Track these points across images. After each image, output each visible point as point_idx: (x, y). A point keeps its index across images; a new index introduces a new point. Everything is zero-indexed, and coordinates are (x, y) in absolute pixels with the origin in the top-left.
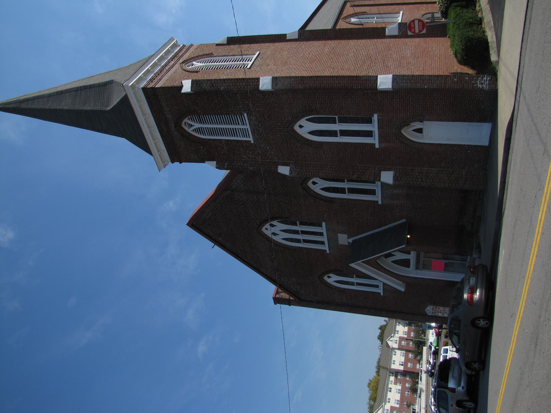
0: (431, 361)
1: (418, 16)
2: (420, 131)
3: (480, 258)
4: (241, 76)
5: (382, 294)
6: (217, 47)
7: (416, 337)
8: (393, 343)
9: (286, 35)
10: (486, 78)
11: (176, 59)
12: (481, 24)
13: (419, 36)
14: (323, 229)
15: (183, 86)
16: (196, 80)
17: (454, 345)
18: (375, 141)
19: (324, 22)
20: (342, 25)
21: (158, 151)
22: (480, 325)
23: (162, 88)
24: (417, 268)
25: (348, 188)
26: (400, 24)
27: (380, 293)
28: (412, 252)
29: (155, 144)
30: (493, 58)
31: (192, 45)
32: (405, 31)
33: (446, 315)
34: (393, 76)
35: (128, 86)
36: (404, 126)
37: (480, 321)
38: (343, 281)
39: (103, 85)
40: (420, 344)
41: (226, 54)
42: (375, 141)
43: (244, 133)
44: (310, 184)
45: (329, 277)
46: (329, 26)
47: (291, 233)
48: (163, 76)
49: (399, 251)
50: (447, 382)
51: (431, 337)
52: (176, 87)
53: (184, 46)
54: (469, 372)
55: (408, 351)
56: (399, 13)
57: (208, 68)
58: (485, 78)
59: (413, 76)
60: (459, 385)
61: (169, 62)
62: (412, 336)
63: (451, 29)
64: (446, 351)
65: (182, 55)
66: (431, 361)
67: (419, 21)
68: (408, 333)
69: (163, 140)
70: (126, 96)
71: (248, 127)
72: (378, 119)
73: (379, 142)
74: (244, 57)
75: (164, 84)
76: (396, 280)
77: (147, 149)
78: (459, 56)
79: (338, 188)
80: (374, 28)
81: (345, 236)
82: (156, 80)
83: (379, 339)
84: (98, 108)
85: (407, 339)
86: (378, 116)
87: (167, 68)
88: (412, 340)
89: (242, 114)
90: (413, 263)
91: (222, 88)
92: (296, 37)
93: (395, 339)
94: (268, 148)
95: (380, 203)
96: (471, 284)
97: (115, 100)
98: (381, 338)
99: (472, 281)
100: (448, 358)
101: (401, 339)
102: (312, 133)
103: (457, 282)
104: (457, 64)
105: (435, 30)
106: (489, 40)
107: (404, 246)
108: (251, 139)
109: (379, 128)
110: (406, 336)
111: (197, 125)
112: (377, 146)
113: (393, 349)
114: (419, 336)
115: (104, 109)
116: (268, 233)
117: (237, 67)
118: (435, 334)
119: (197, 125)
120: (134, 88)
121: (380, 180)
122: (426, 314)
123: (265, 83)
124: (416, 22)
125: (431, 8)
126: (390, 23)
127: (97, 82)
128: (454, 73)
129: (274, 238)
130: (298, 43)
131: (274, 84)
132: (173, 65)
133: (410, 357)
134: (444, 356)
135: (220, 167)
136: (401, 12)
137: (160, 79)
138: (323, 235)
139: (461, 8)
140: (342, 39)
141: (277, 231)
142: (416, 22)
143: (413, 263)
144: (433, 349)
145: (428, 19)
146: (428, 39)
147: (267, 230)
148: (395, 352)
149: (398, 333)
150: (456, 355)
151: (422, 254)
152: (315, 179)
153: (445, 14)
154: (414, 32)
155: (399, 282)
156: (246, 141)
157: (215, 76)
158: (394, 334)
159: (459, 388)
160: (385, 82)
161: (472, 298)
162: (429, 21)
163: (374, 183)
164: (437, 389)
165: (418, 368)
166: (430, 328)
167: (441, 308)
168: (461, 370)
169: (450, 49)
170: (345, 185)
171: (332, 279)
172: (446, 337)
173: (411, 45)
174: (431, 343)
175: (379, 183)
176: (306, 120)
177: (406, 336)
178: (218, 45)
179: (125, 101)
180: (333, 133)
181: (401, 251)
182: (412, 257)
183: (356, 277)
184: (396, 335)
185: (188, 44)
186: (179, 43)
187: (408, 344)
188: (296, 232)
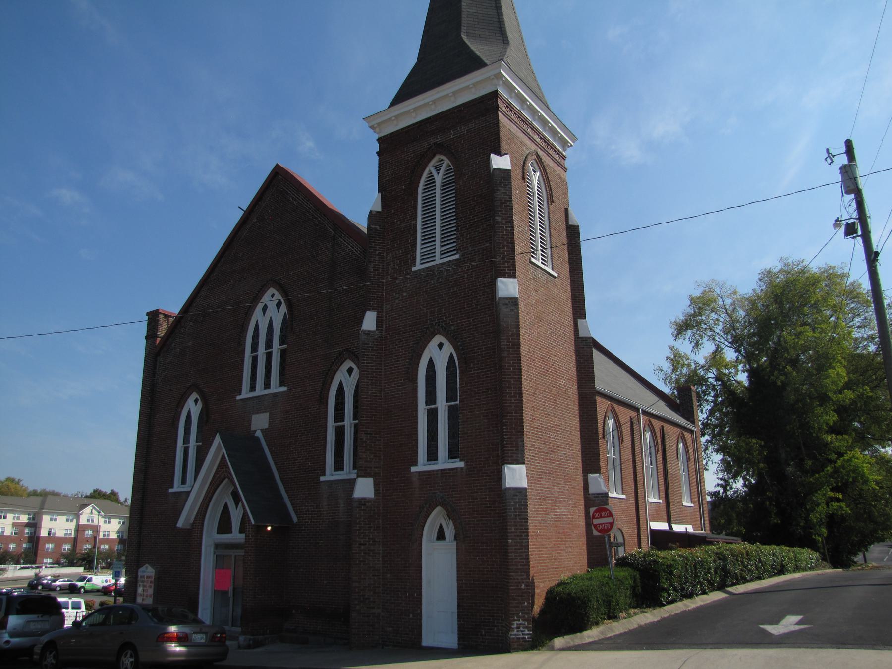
0: (58, 583)
1: (619, 523)
2: (441, 536)
3: (239, 647)
4: (518, 249)
5: (171, 490)
6: (563, 210)
7: (100, 553)
8: (89, 515)
9: (584, 317)
10: (527, 634)
11: (543, 145)
12: (609, 618)
13: (589, 525)
14: (275, 388)
15: (501, 156)
16: (510, 177)
17: (85, 618)
18: (422, 465)
19: (605, 377)
20: (602, 406)
21: (397, 117)
22: (123, 658)
23: (497, 122)
24: (217, 546)
25: (344, 426)
26: (606, 495)
27: (172, 487)
28: (243, 536)
29: (408, 112)
30: (558, 642)
31: (565, 170)
32: (597, 504)
33: (139, 600)
34: (525, 489)
35: (500, 67)
36: (447, 510)
37: (131, 656)
38: (190, 424)
39: (501, 28)
40: (88, 562)
41: (553, 224)
42: (422, 465)
43: (429, 255)
44: (349, 364)
45: (196, 401)
46: (599, 386)
47: (267, 336)
48: (515, 124)
49: (245, 515)
50: (18, 613)
51: (101, 579)
52: (499, 146)
53: (564, 158)
54: (37, 649)
55: (75, 541)
56: (623, 493)
57: (530, 195)
58: (527, 632)
59: (526, 520)
60: (12, 635)
61: (539, 134)
62: (102, 547)
63: (600, 574)
64: (76, 606)
65: (550, 153)
66: (58, 583)
67: (612, 524)
68: (106, 540)
69: (414, 125)
70: (485, 65)
71: (438, 261)
72: (456, 469)
73: (420, 472)
74: (549, 250)
75: (504, 126)
76: (195, 513)
77: (401, 97)
78: (561, 588)
79: (343, 409)
80: (598, 455)
81: (266, 426)
82: (509, 113)
83: (95, 491)
84: (465, 20)
85: (95, 538)
86: (462, 468)
87: (529, 131)
88: (94, 547)
89: (457, 250)
90: (225, 538)
91: (499, 219)
92: (582, 334)
93: (96, 518)
94: (405, 294)
95: (322, 479)
96: (194, 636)
97: (477, 48)
98: (97, 495)
99: (199, 638)
100: (64, 610)
101: (96, 529)
102: (431, 365)
103: (196, 614)
104: (548, 588)
105: (598, 549)
106: (586, 633)
107: (253, 522)
108: (418, 266)
109: (443, 471)
110: (101, 536)
111: (438, 179)
112: (413, 469)
113: (78, 517)
114: (102, 559)
115: (464, 29)
116: (266, 298)
117: (532, 241)
118: (106, 584)
119: (438, 179)
120: (497, 79)
121: (358, 476)
122: (139, 566)
123: (507, 287)
124: (610, 520)
125: (631, 541)
126: (607, 481)
127: (506, 18)
128: (533, 583)
129: (260, 307)
130: (573, 338)
131: (507, 302)
132: (533, 141)
133: (64, 546)
134: (67, 603)
135: (373, 217)
136: (624, 497)
137: (511, 120)
138: (265, 388)
139: (631, 587)
140: (580, 405)
141: (269, 312)
142: (610, 520)
143: (225, 538)
144: (80, 584)
145: (615, 538)
146: (584, 540)
147: (271, 296)
148: (72, 520)
149: (105, 522)
150: (68, 624)
151: (241, 552)
152: (356, 371)
153: (623, 563)
154: (594, 518)
155: (193, 518)
156: (414, 259)
157: (516, 206)
158: (104, 517)
159: (7, 635)
160: (516, 476)
161: (171, 639)
162: (612, 539)
163: (354, 468)
164: (4, 598)
165: (45, 561)
166: (117, 576)
167: (151, 591)
168: (41, 635)
169: (570, 574)
170: (349, 421)
171: (193, 407)
172: (102, 604)
173: (574, 514)
174: (90, 580)
175: (354, 476)
176: (451, 354)
177: (101, 536)
178: (567, 210)
179: (477, 64)
180: (431, 398)
181: (245, 516)
182: (236, 536)
183: (198, 447)
184: (102, 520)
185: (567, 163)
186: (569, 150)
187: (87, 541)
188: (269, 344)
